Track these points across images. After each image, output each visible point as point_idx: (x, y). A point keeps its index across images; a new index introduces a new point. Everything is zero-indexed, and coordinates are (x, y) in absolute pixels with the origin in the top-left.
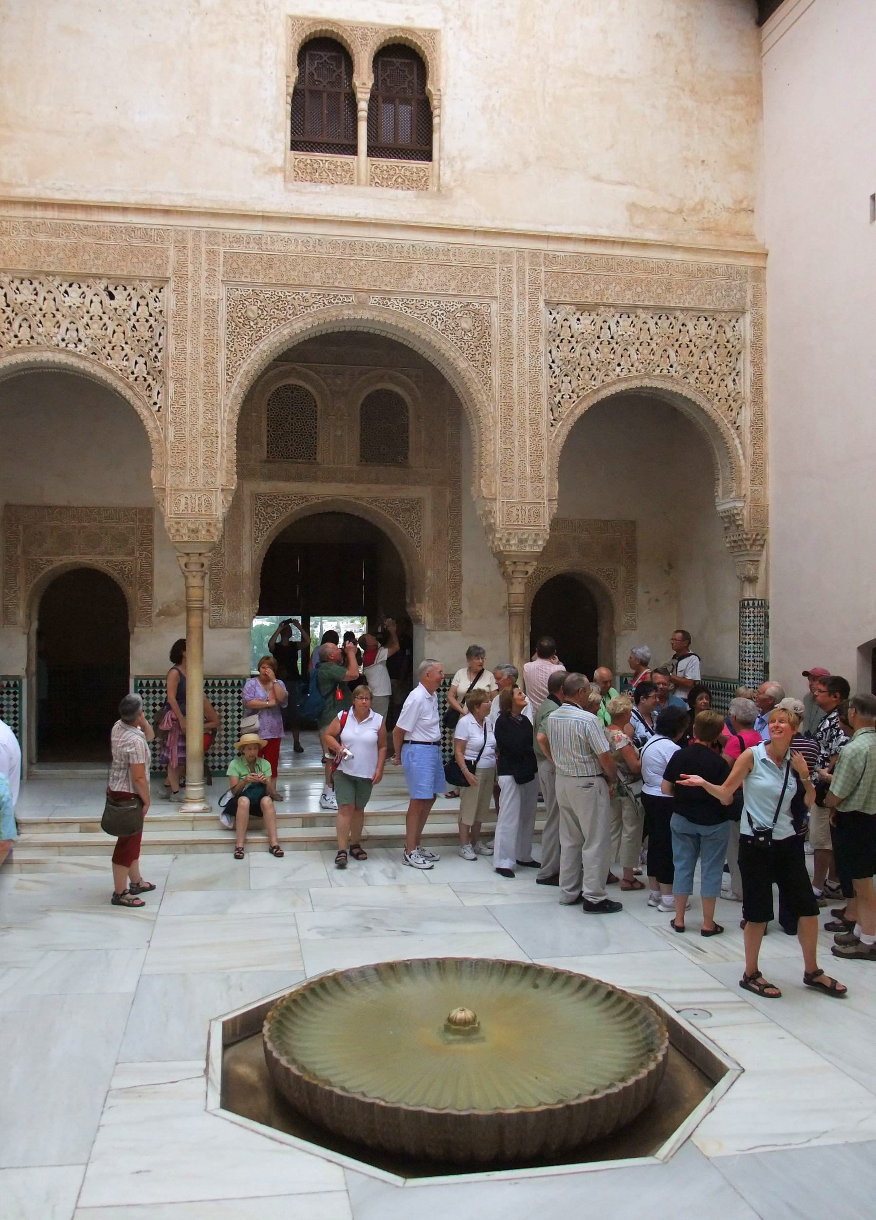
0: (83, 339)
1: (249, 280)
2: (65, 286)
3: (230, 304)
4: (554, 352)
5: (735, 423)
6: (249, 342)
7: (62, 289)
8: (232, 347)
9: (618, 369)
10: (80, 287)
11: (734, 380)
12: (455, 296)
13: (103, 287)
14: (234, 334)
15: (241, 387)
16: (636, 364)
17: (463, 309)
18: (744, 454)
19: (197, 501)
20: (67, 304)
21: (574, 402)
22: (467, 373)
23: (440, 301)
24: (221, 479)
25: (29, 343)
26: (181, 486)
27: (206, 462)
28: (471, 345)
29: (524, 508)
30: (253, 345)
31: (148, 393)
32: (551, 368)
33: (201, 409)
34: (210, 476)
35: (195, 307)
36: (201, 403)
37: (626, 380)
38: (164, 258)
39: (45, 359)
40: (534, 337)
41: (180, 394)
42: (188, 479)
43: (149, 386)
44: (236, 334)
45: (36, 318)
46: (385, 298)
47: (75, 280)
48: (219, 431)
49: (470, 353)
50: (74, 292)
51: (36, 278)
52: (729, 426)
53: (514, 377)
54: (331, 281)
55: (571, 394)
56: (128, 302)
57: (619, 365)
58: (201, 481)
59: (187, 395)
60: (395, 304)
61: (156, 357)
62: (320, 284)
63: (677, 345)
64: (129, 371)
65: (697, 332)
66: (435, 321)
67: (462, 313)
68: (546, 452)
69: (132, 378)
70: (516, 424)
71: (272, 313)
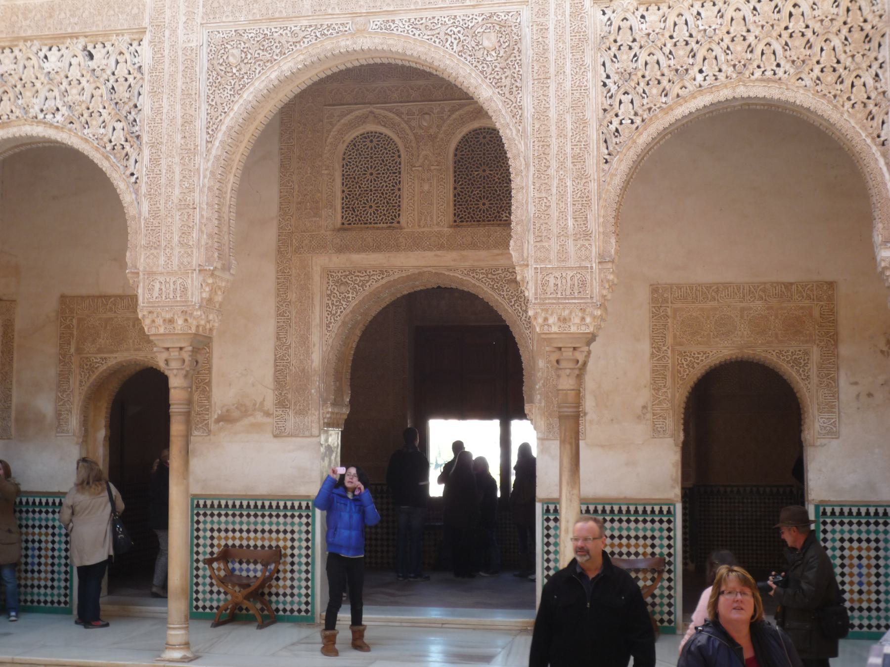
0: (60, 108)
1: (230, 19)
2: (45, 49)
3: (211, 50)
4: (608, 64)
5: (879, 136)
6: (232, 93)
7: (41, 54)
8: (212, 100)
9: (700, 77)
10: (59, 50)
11: (877, 75)
12: (474, 6)
13: (80, 47)
14: (215, 85)
15: (223, 148)
16: (724, 68)
17: (485, 21)
19: (172, 285)
20: (46, 70)
21: (637, 128)
22: (493, 104)
23: (455, 16)
24: (197, 258)
25: (9, 118)
26: (154, 269)
27: (182, 239)
28: (496, 67)
29: (564, 275)
31: (125, 163)
32: (605, 85)
33: (177, 177)
34: (186, 255)
35: (173, 58)
36: (177, 170)
37: (711, 89)
38: (141, 6)
39: (23, 135)
40: (578, 48)
41: (155, 161)
42: (162, 260)
43: (127, 154)
44: (217, 84)
45: (16, 89)
46: (388, 21)
47: (56, 41)
48: (197, 201)
49: (494, 78)
50: (53, 55)
51: (16, 46)
52: (869, 141)
53: (551, 103)
54: (323, 8)
55: (633, 117)
56: (105, 62)
57: (701, 71)
58: (175, 261)
59: (163, 161)
61: (135, 121)
62: (310, 14)
63: (785, 34)
64: (106, 139)
65: (816, 13)
66: (449, 42)
67: (484, 27)
68: (594, 198)
69: (109, 147)
70: (554, 164)
71: (257, 55)
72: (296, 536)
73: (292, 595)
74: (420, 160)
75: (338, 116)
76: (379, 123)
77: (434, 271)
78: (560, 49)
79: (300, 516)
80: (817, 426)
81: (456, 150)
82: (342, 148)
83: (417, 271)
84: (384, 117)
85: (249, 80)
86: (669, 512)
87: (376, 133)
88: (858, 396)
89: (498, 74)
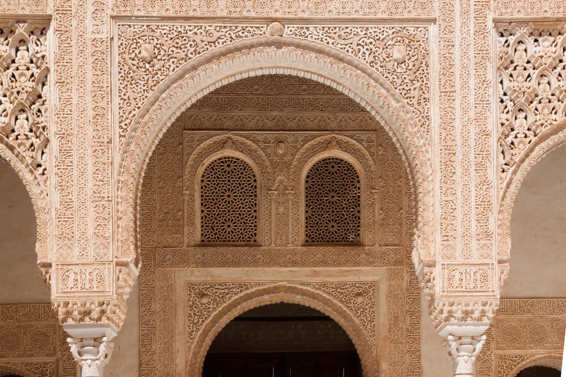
28: (405, 78)
30: (150, 91)
40: (480, 65)
66: (361, 52)
74: (275, 185)
75: (198, 140)
76: (236, 149)
77: (288, 285)
78: (465, 65)
81: (308, 177)
82: (201, 170)
84: (241, 143)
85: (163, 77)
87: (233, 158)
89: (407, 86)
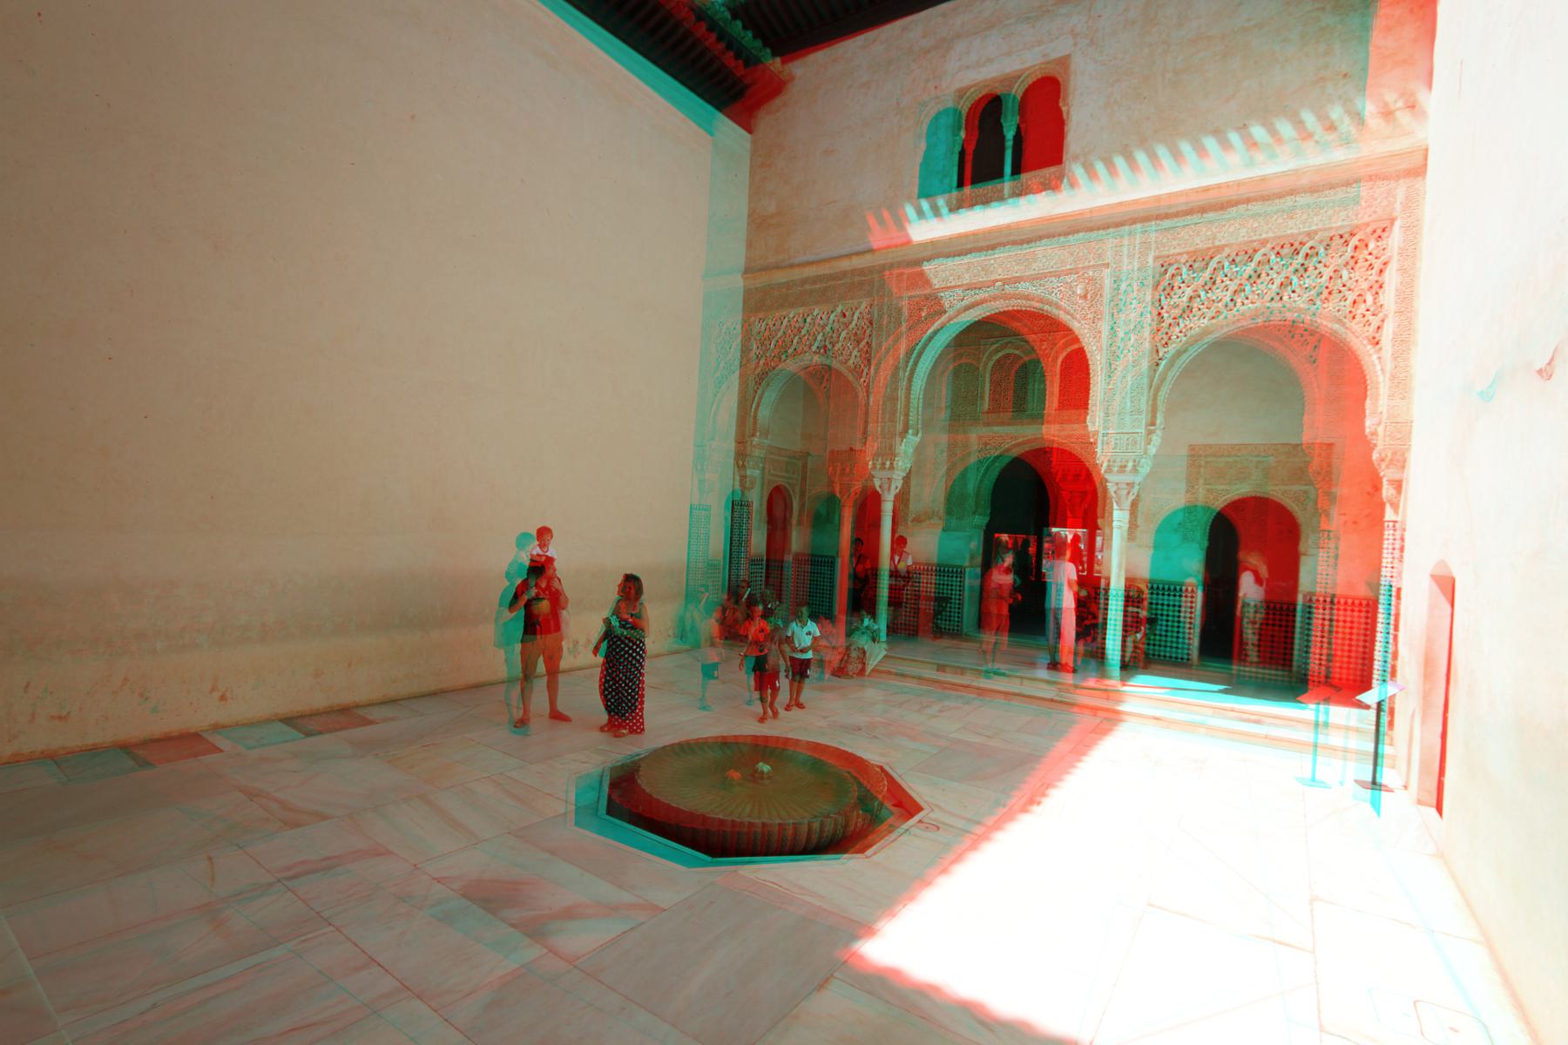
18: (1382, 370)
32: (1159, 314)
60: (1024, 287)
72: (954, 588)
73: (950, 621)
79: (957, 577)
80: (1310, 542)
81: (1062, 362)
82: (991, 364)
83: (1033, 437)
86: (1192, 591)
88: (1345, 523)
